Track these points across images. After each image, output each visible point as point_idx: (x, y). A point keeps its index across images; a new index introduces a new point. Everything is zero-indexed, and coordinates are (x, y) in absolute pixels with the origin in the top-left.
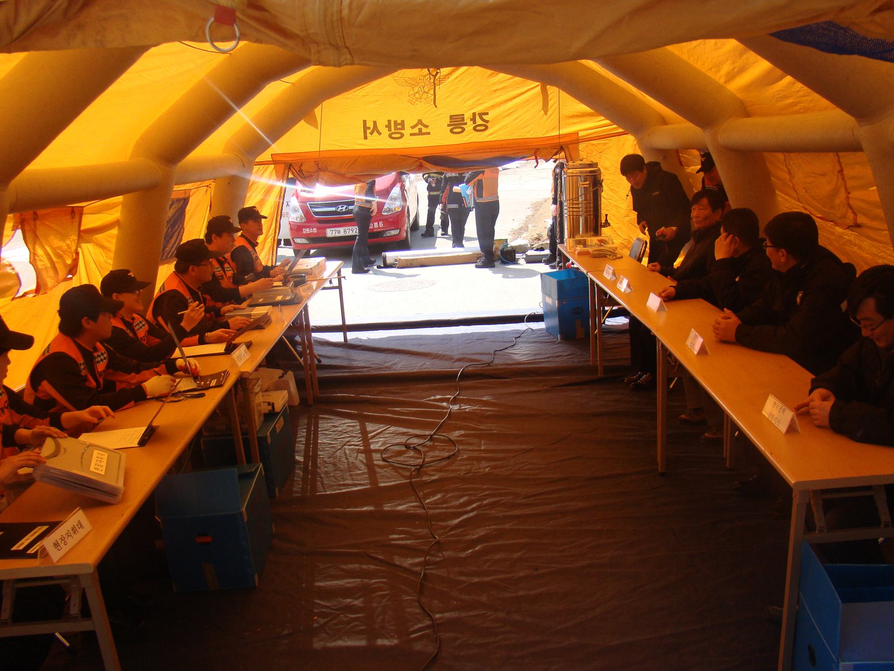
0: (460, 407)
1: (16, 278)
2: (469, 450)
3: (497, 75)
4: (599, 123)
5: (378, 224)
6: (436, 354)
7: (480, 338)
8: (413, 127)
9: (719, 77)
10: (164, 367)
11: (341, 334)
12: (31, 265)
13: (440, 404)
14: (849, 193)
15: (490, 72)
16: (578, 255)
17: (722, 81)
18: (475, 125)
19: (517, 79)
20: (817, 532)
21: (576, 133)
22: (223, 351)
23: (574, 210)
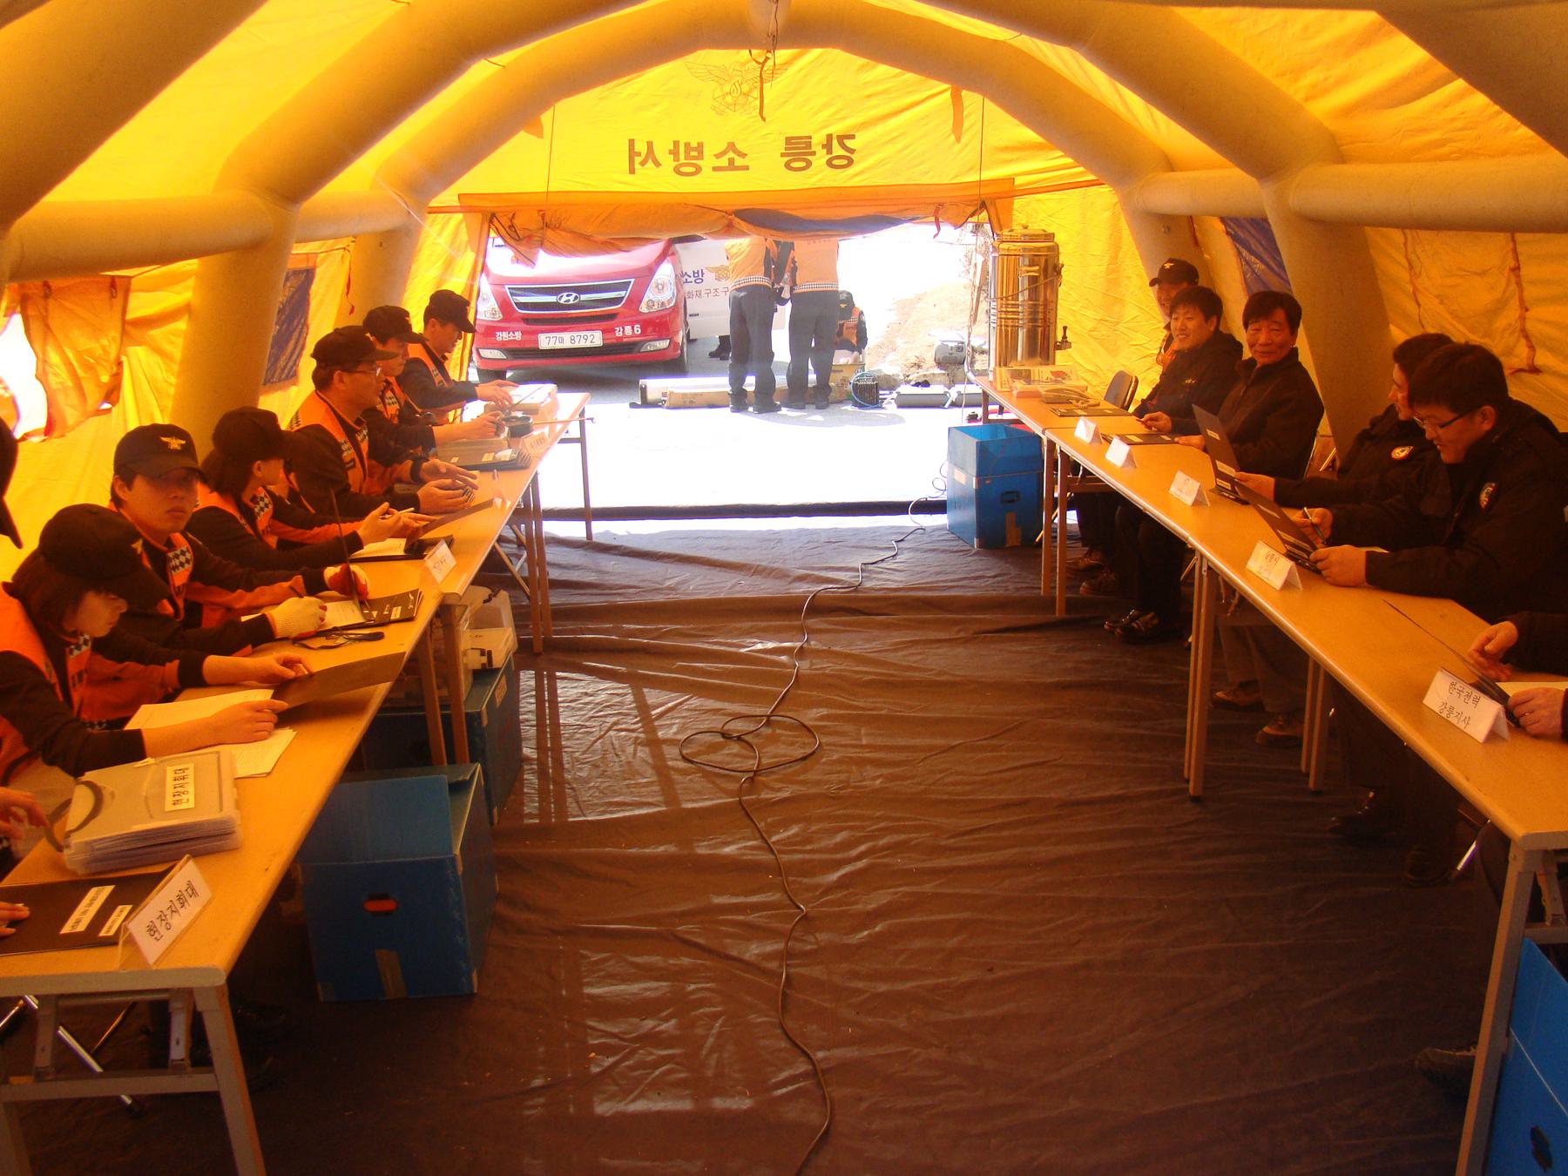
0: (812, 664)
1: (11, 404)
2: (842, 746)
3: (873, 68)
4: (1055, 163)
5: (633, 328)
6: (758, 566)
7: (833, 540)
8: (718, 156)
9: (1296, 90)
10: (301, 580)
11: (582, 524)
12: (38, 382)
13: (775, 657)
14: (1527, 310)
15: (861, 61)
16: (1018, 397)
17: (1299, 97)
18: (831, 156)
19: (909, 76)
20: (1548, 923)
21: (1011, 179)
22: (401, 552)
23: (1009, 316)
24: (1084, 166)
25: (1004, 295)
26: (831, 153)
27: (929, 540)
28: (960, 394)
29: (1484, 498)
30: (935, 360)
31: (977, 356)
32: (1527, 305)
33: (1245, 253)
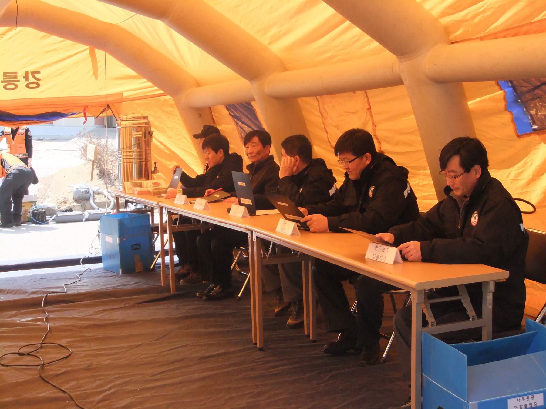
6: (9, 290)
9: (264, 40)
14: (376, 126)
15: (43, 34)
17: (266, 43)
19: (69, 42)
24: (157, 86)
25: (125, 147)
26: (28, 81)
27: (95, 273)
28: (90, 214)
29: (371, 193)
30: (74, 199)
31: (96, 196)
32: (376, 124)
33: (240, 123)
